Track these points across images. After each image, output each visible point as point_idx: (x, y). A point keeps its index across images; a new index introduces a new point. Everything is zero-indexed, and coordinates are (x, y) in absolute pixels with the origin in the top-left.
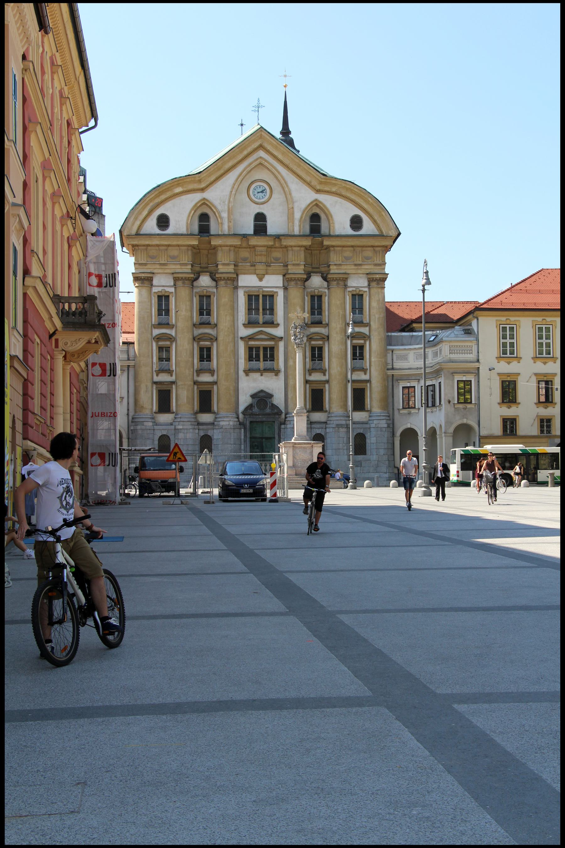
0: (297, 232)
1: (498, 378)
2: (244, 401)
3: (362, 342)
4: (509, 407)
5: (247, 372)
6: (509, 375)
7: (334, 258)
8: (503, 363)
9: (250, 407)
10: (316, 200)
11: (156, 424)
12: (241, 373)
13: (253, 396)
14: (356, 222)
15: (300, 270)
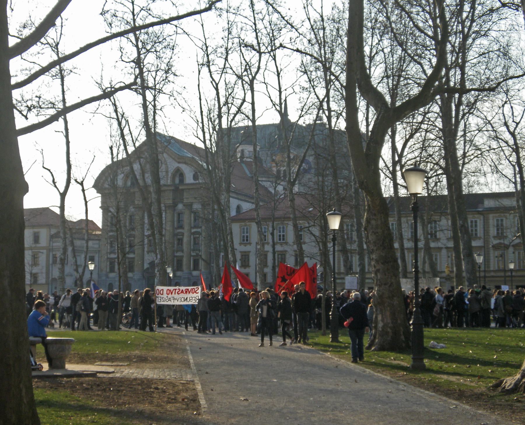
0: (169, 183)
1: (240, 254)
2: (146, 266)
3: (198, 236)
4: (245, 268)
5: (148, 252)
6: (245, 252)
7: (186, 195)
8: (242, 246)
9: (148, 269)
10: (178, 167)
11: (107, 277)
12: (145, 253)
13: (150, 264)
14: (195, 177)
15: (170, 202)
